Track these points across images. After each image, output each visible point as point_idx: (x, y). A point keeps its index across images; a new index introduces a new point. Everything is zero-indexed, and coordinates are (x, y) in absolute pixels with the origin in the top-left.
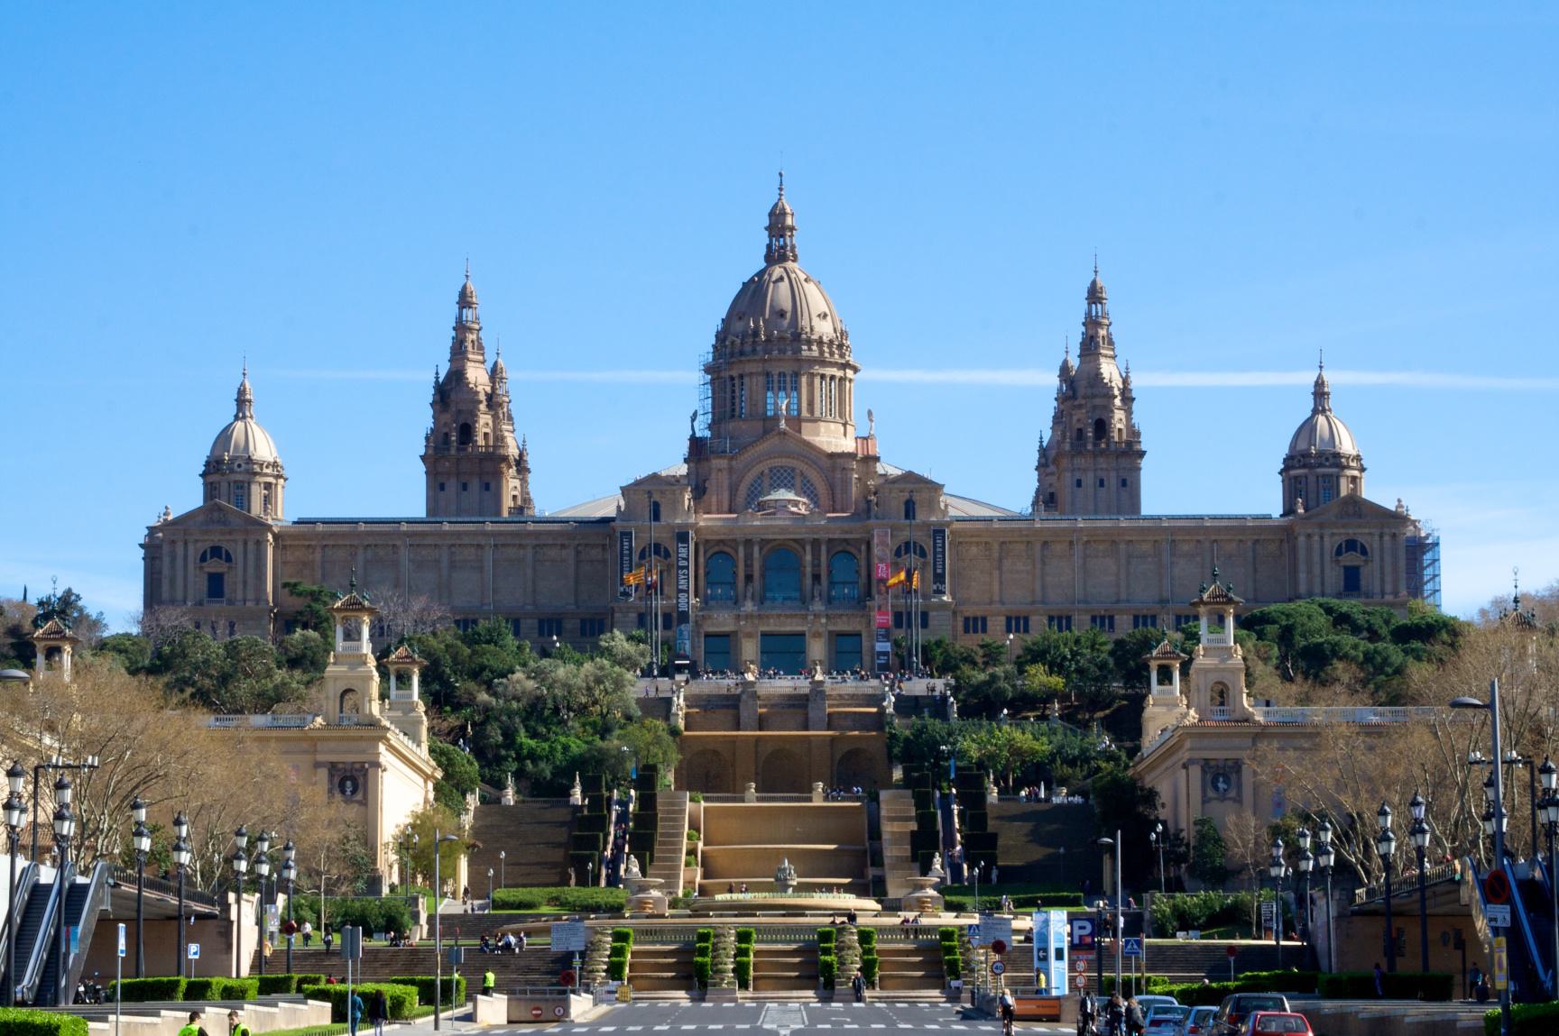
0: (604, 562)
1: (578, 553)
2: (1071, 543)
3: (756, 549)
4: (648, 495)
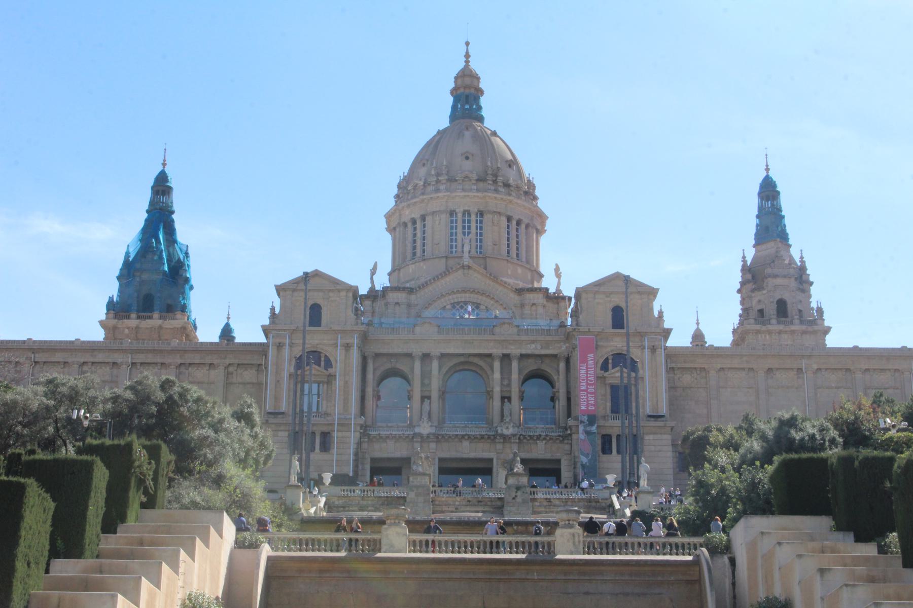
0: (260, 384)
1: (228, 374)
2: (801, 369)
3: (435, 364)
4: (308, 299)
